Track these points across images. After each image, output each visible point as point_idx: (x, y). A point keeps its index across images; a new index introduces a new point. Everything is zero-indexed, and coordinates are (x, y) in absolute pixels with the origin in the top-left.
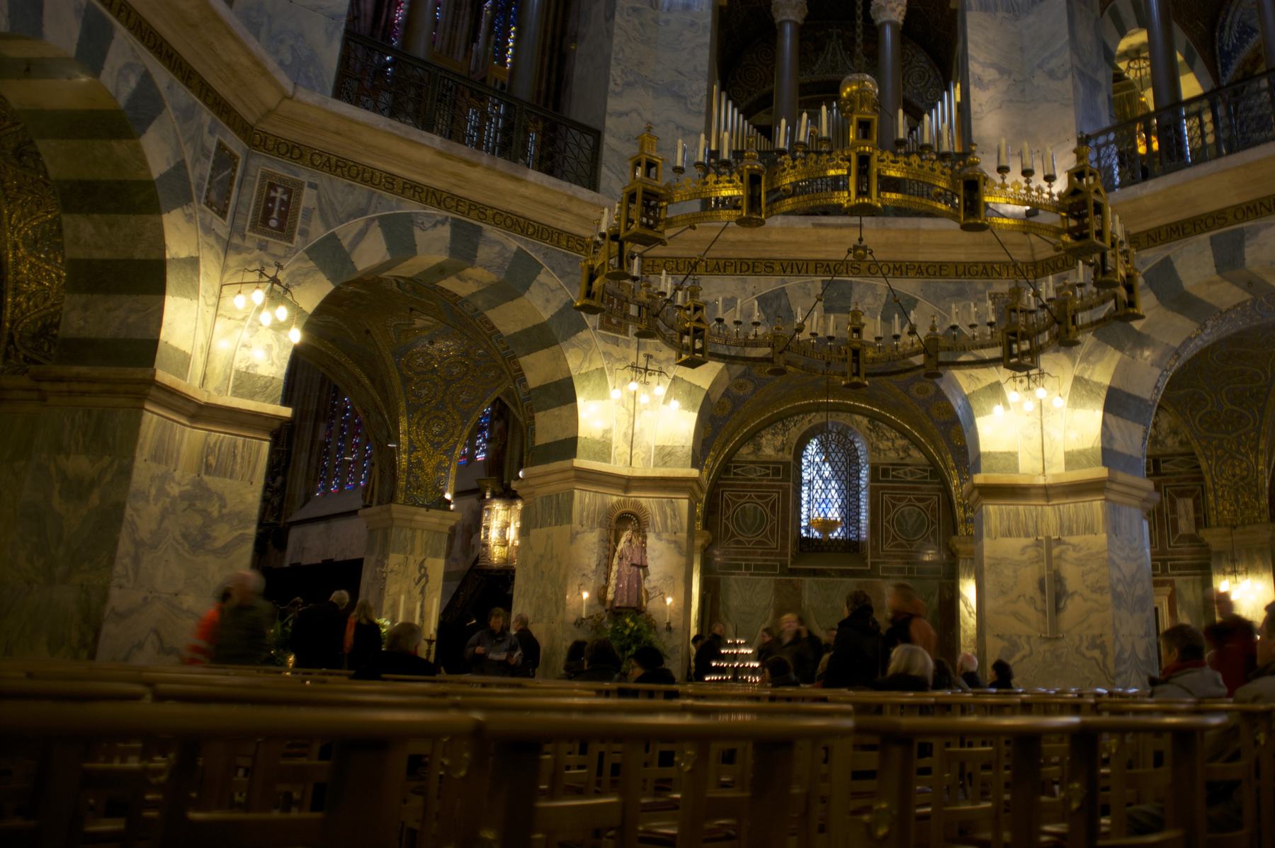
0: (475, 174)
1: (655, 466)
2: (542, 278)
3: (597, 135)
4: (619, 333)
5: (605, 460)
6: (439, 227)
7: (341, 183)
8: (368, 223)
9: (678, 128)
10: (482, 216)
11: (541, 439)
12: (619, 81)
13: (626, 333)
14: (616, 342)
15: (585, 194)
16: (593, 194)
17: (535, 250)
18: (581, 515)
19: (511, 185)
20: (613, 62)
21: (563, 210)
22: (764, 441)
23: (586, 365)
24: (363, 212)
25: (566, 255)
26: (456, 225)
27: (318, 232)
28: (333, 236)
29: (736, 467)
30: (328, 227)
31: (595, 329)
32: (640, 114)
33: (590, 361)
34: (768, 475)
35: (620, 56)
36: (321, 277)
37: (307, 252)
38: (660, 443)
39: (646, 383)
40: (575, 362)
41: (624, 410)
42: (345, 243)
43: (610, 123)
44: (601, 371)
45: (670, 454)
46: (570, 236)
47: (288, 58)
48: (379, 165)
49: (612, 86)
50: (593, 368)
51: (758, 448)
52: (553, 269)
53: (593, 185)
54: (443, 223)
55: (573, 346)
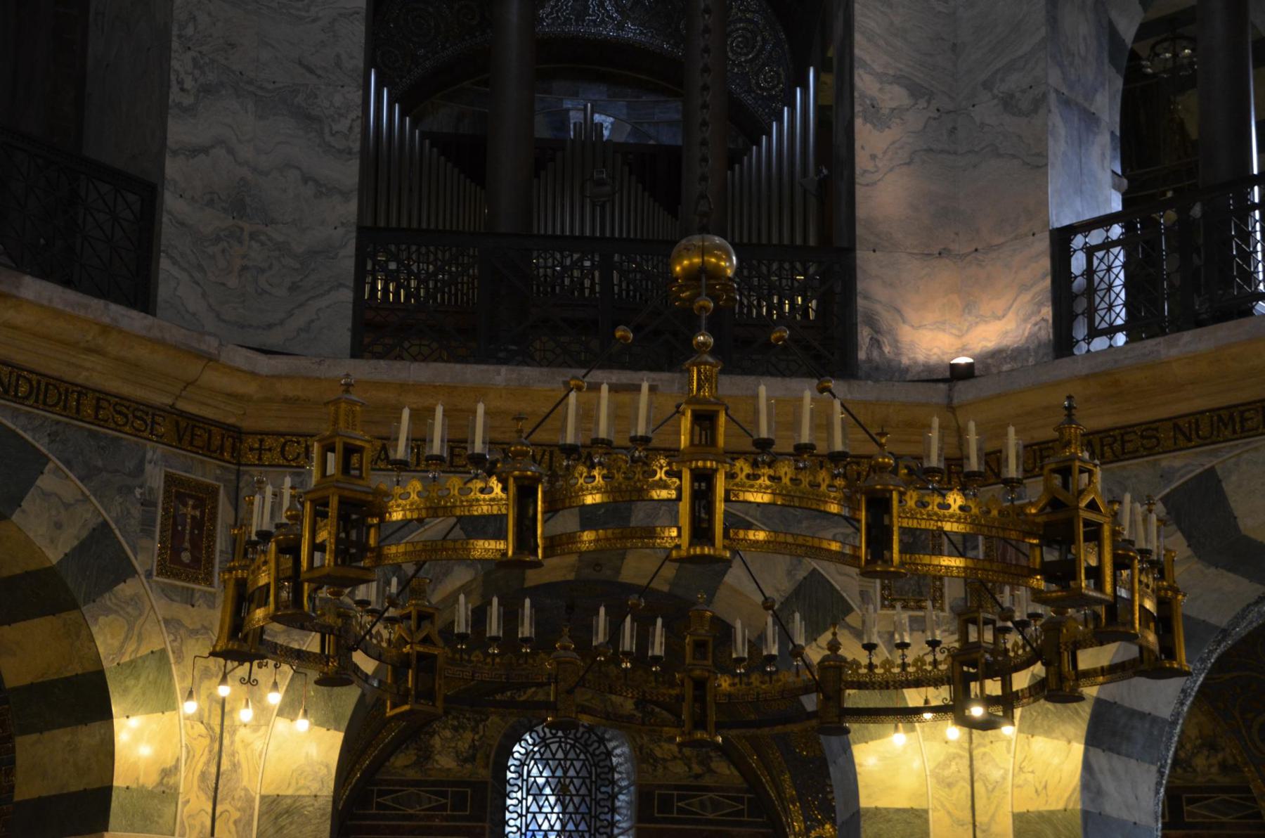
2: (46, 481)
3: (149, 194)
4: (196, 580)
9: (306, 179)
11: (27, 788)
12: (189, 84)
13: (208, 580)
14: (189, 599)
15: (134, 320)
16: (149, 320)
20: (175, 44)
21: (89, 350)
22: (437, 741)
23: (131, 647)
25: (93, 435)
29: (381, 794)
31: (149, 575)
32: (231, 151)
33: (140, 639)
34: (443, 807)
35: (190, 31)
38: (271, 790)
39: (249, 681)
40: (109, 641)
41: (201, 729)
43: (173, 168)
44: (161, 657)
45: (288, 812)
46: (102, 397)
49: (175, 95)
50: (144, 651)
51: (426, 755)
52: (68, 463)
53: (141, 296)
55: (108, 611)
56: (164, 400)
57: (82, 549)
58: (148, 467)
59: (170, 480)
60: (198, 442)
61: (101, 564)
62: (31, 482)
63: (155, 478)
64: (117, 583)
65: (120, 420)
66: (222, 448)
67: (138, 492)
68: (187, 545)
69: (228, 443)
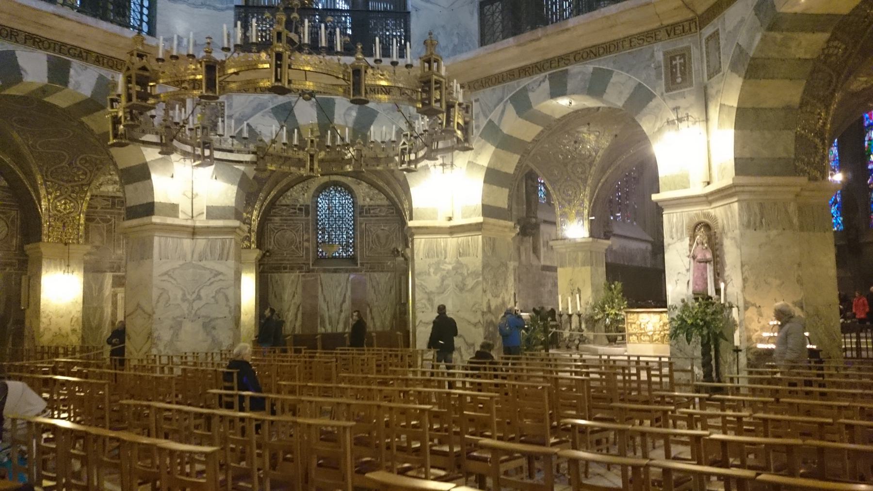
0: (544, 43)
1: (719, 180)
2: (614, 79)
5: (685, 188)
6: (542, 85)
7: (488, 90)
8: (505, 106)
10: (567, 62)
17: (603, 63)
18: (671, 232)
19: (565, 36)
24: (501, 100)
26: (551, 77)
27: (483, 123)
28: (490, 121)
30: (486, 116)
33: (662, 119)
36: (489, 145)
37: (480, 136)
42: (496, 122)
45: (724, 169)
47: (456, 41)
48: (503, 69)
52: (622, 69)
54: (544, 81)
56: (656, 25)
57: (632, 96)
58: (656, 54)
59: (665, 54)
60: (678, 32)
61: (641, 98)
62: (608, 82)
63: (660, 56)
64: (648, 102)
65: (641, 42)
66: (690, 30)
67: (653, 65)
68: (679, 75)
69: (693, 26)
